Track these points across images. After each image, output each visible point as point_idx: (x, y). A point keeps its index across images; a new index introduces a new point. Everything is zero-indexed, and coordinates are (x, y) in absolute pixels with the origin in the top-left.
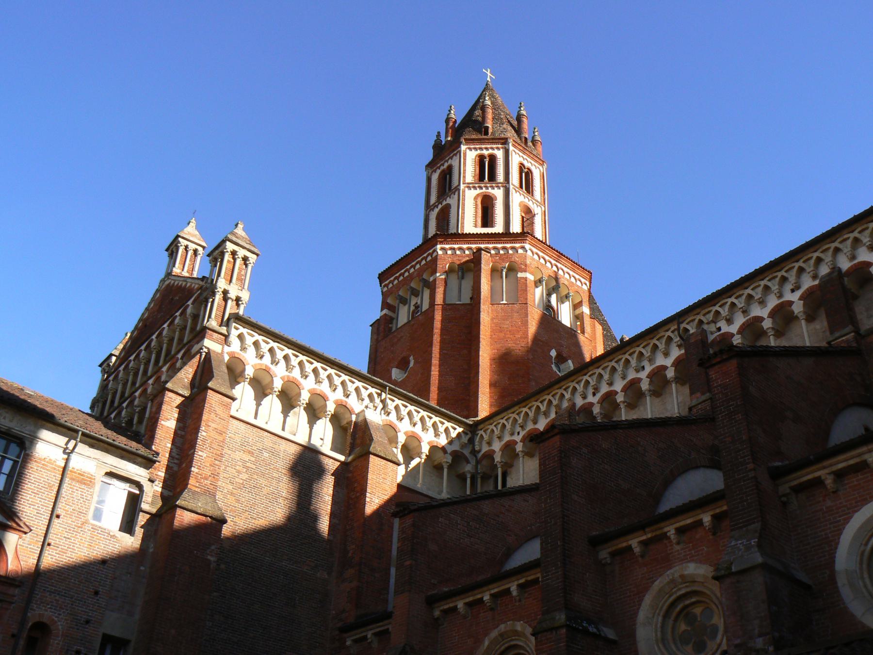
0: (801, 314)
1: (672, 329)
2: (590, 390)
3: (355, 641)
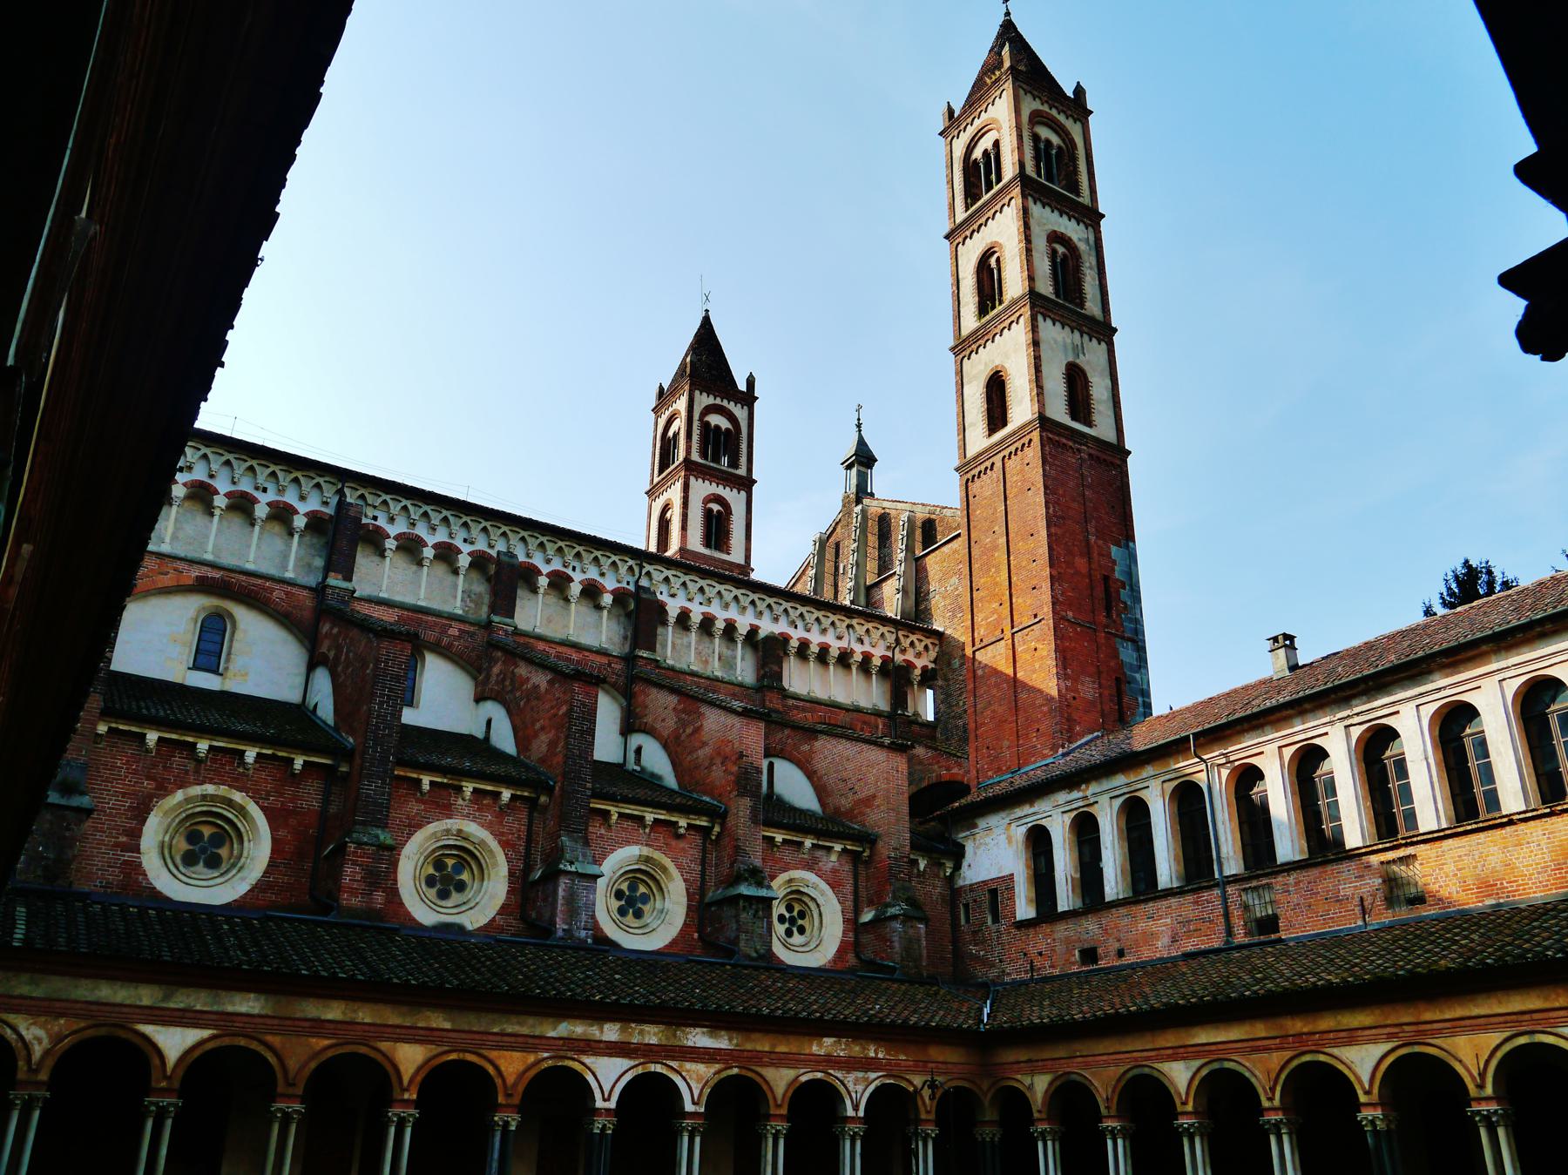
0: (464, 569)
1: (327, 479)
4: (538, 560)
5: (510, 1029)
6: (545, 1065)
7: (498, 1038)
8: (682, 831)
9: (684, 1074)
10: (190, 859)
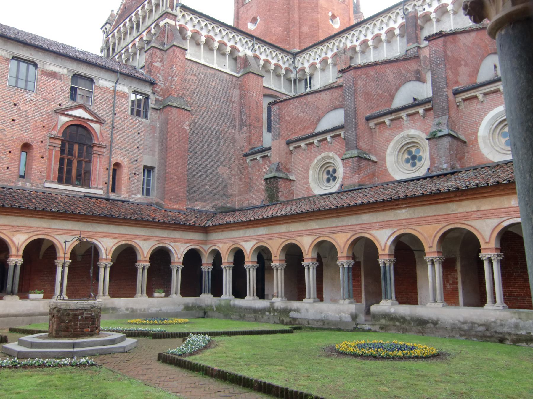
2: (355, 39)
3: (251, 160)
5: (339, 225)
7: (335, 229)
10: (328, 180)
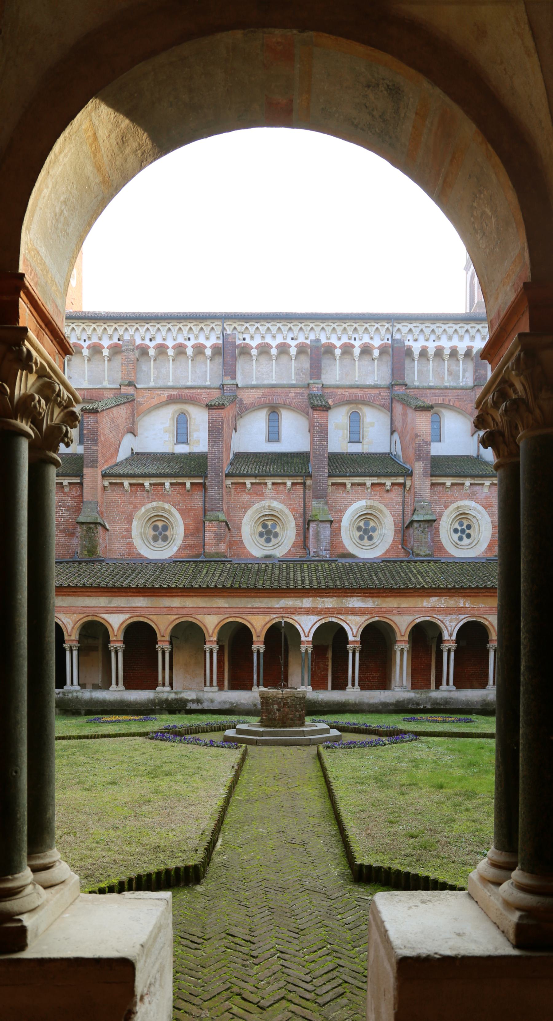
4: (333, 340)
5: (256, 605)
6: (274, 621)
7: (251, 610)
8: (388, 488)
9: (348, 622)
